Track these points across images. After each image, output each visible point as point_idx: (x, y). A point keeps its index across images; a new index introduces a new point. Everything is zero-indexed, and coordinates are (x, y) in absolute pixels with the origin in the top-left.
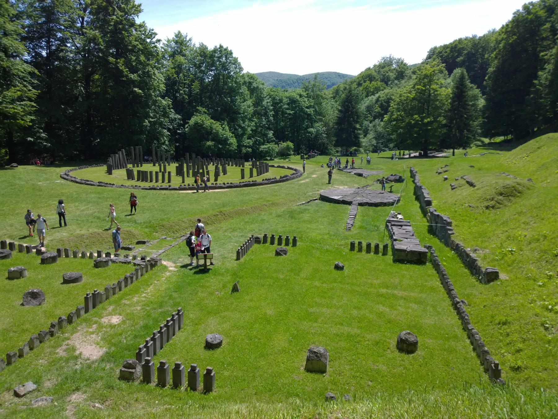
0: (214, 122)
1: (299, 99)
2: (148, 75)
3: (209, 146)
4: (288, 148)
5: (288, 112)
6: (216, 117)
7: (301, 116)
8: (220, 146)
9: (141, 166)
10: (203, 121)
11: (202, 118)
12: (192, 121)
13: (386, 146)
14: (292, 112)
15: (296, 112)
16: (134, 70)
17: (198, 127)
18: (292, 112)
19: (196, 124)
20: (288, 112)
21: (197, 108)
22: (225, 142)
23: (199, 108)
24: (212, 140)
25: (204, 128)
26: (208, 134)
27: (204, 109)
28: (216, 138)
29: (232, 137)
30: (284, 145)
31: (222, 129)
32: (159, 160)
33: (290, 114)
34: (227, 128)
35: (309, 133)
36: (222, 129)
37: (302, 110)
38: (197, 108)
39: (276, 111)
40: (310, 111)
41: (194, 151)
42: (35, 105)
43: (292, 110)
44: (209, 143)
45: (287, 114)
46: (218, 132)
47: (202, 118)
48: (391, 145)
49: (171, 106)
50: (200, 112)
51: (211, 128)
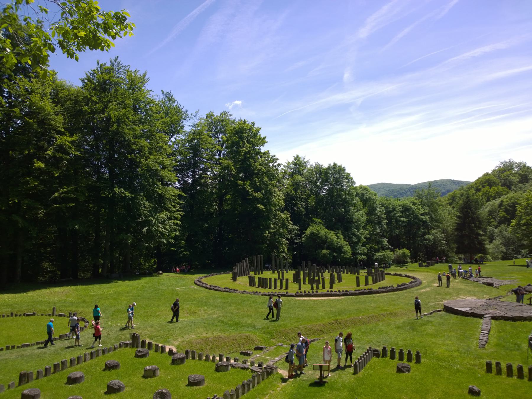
0: (329, 232)
1: (413, 207)
3: (325, 254)
4: (404, 255)
5: (402, 219)
6: (330, 227)
7: (416, 223)
8: (335, 254)
9: (262, 273)
11: (317, 228)
12: (308, 231)
13: (518, 253)
14: (406, 220)
17: (314, 236)
18: (406, 220)
19: (312, 233)
20: (402, 219)
21: (313, 219)
22: (339, 250)
23: (315, 219)
24: (327, 249)
25: (319, 237)
26: (323, 243)
27: (319, 220)
28: (332, 247)
29: (346, 245)
30: (400, 252)
31: (337, 238)
32: (278, 268)
33: (403, 222)
34: (342, 237)
35: (426, 240)
36: (337, 238)
37: (416, 217)
38: (313, 219)
39: (390, 219)
40: (426, 218)
41: (311, 259)
42: (179, 222)
44: (325, 251)
45: (400, 221)
47: (317, 228)
48: (523, 252)
50: (316, 223)
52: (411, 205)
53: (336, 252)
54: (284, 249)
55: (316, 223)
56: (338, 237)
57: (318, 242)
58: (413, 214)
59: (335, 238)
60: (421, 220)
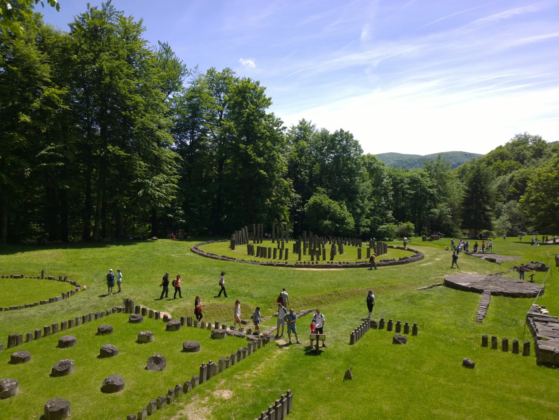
0: (333, 202)
1: (421, 179)
2: (273, 158)
3: (327, 225)
4: (408, 229)
5: (409, 191)
6: (334, 197)
7: (423, 195)
8: (338, 226)
11: (321, 198)
12: (311, 201)
13: (524, 230)
14: (413, 192)
15: (418, 191)
16: (260, 155)
17: (317, 206)
18: (413, 192)
19: (315, 203)
20: (409, 191)
21: (317, 188)
22: (342, 221)
23: (319, 188)
24: (330, 219)
25: (322, 207)
26: (325, 213)
27: (323, 190)
29: (350, 216)
30: (405, 225)
31: (339, 208)
33: (410, 194)
34: (345, 207)
35: (432, 213)
36: (339, 208)
37: (423, 190)
38: (317, 188)
41: (312, 229)
43: (413, 190)
44: (327, 222)
45: (407, 193)
47: (321, 198)
48: (530, 229)
49: (292, 186)
50: (319, 192)
52: (420, 177)
53: (338, 223)
55: (319, 192)
56: (342, 207)
57: (320, 212)
58: (420, 186)
59: (338, 208)
60: (428, 193)
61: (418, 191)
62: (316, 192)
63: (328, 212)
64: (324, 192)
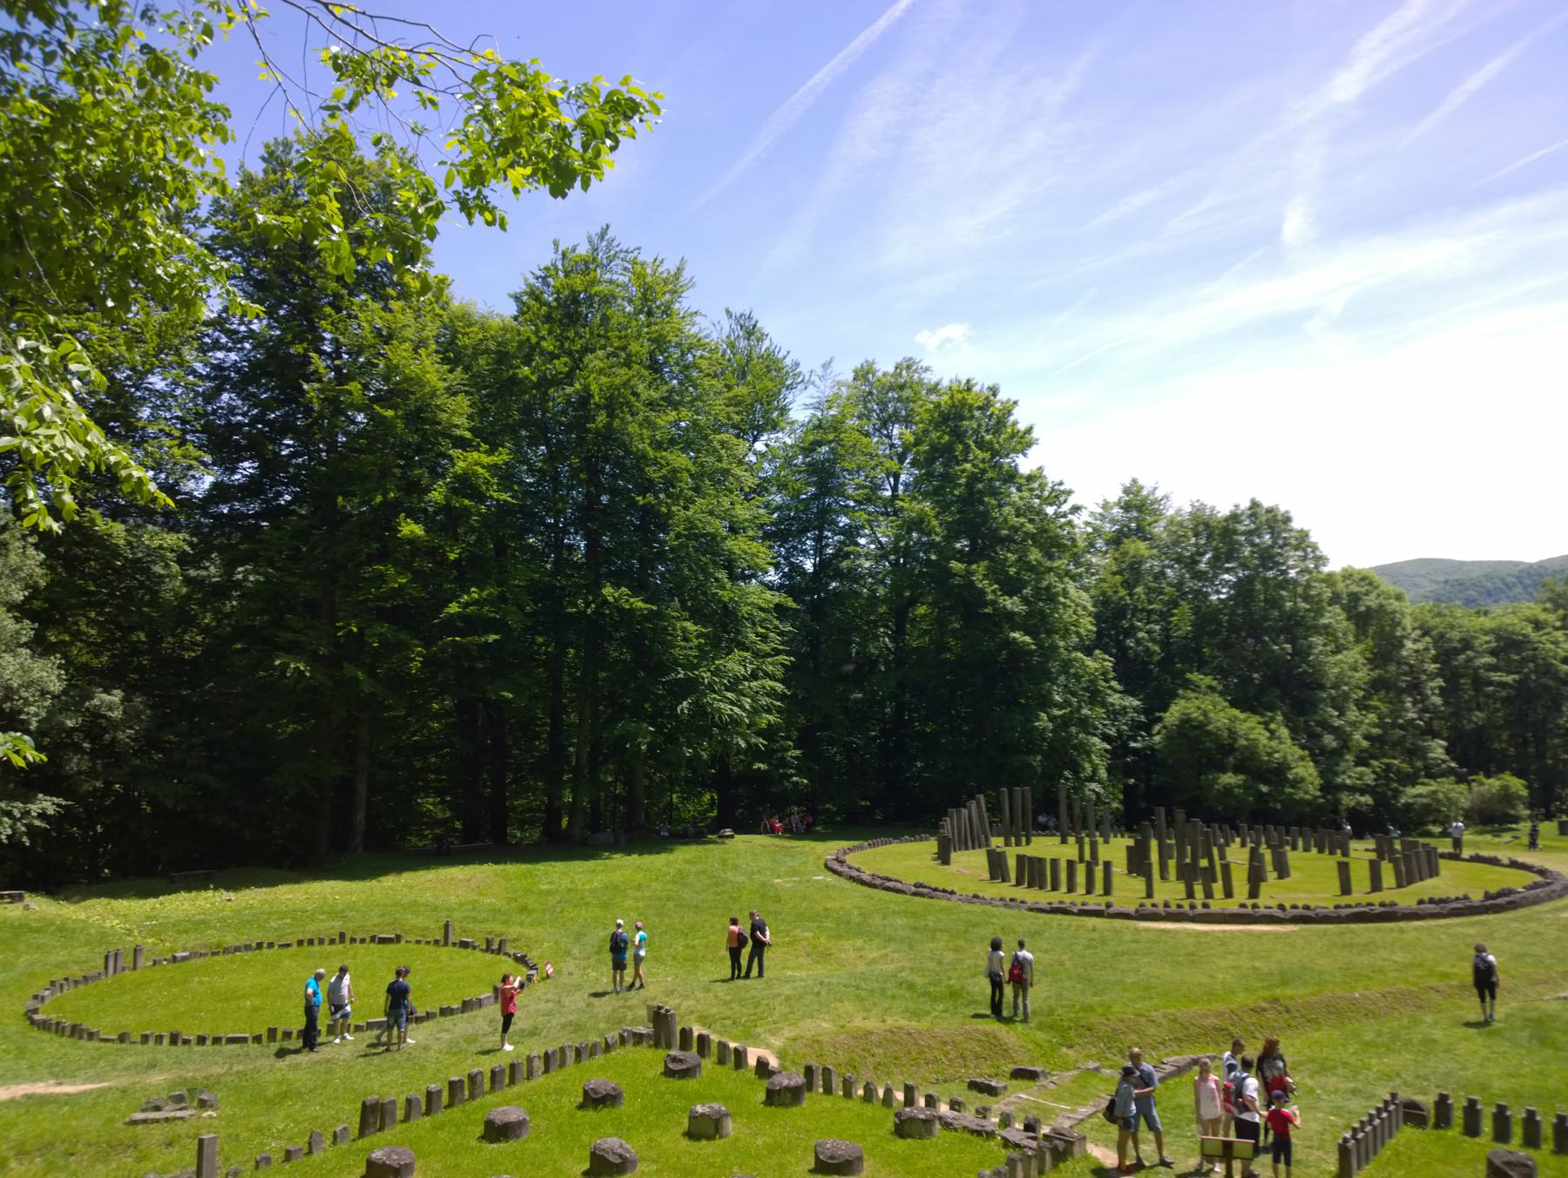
0: (1242, 716)
1: (1534, 636)
2: (1050, 596)
3: (1228, 789)
4: (1506, 796)
5: (1496, 677)
6: (1244, 700)
7: (1547, 688)
8: (1264, 789)
9: (1028, 842)
10: (1205, 714)
11: (1202, 704)
12: (1173, 714)
14: (1509, 679)
15: (1527, 676)
16: (1011, 587)
17: (1190, 731)
18: (1509, 679)
19: (1186, 721)
20: (1496, 677)
21: (1189, 676)
22: (1278, 774)
23: (1195, 677)
25: (1209, 733)
26: (1223, 751)
27: (1208, 680)
29: (1302, 758)
30: (1492, 784)
32: (1078, 828)
33: (1503, 685)
34: (1284, 732)
37: (1547, 670)
38: (1189, 676)
41: (1181, 801)
42: (779, 687)
43: (1509, 673)
44: (1228, 778)
45: (1491, 683)
46: (1256, 747)
47: (1202, 704)
49: (1112, 675)
50: (1196, 688)
51: (1232, 733)
52: (1529, 629)
54: (1095, 771)
55: (1196, 688)
56: (1272, 732)
58: (1533, 659)
59: (1261, 736)
61: (1527, 676)
62: (1186, 688)
63: (1230, 749)
64: (1212, 689)
